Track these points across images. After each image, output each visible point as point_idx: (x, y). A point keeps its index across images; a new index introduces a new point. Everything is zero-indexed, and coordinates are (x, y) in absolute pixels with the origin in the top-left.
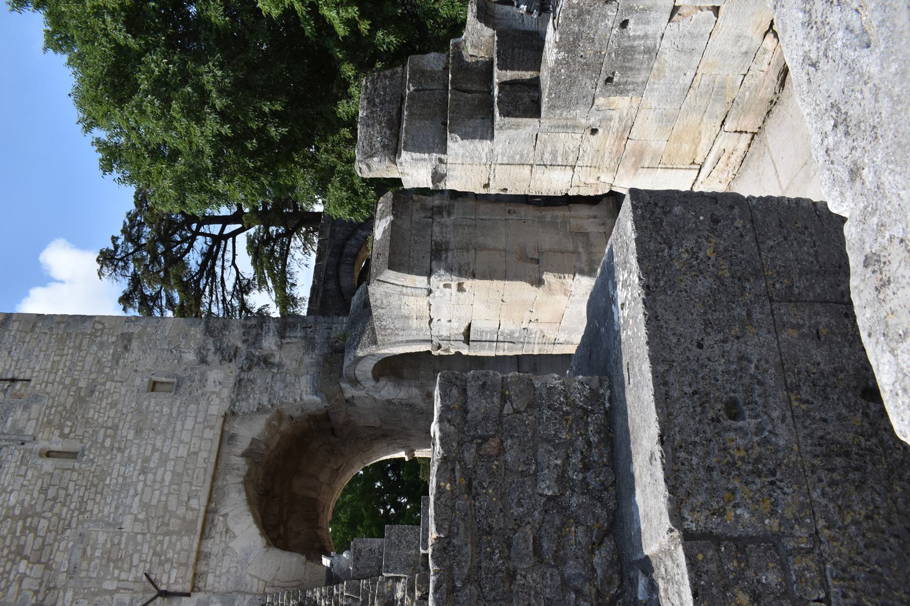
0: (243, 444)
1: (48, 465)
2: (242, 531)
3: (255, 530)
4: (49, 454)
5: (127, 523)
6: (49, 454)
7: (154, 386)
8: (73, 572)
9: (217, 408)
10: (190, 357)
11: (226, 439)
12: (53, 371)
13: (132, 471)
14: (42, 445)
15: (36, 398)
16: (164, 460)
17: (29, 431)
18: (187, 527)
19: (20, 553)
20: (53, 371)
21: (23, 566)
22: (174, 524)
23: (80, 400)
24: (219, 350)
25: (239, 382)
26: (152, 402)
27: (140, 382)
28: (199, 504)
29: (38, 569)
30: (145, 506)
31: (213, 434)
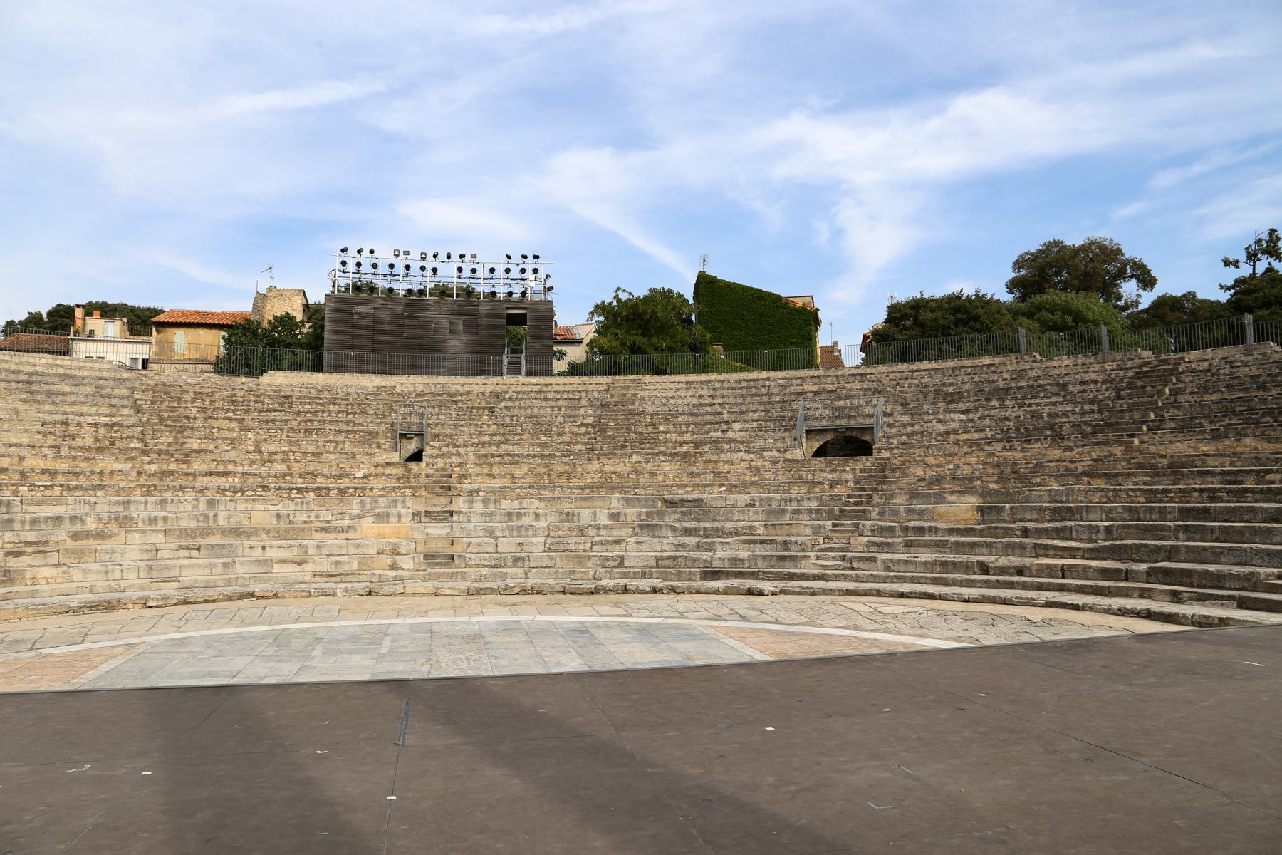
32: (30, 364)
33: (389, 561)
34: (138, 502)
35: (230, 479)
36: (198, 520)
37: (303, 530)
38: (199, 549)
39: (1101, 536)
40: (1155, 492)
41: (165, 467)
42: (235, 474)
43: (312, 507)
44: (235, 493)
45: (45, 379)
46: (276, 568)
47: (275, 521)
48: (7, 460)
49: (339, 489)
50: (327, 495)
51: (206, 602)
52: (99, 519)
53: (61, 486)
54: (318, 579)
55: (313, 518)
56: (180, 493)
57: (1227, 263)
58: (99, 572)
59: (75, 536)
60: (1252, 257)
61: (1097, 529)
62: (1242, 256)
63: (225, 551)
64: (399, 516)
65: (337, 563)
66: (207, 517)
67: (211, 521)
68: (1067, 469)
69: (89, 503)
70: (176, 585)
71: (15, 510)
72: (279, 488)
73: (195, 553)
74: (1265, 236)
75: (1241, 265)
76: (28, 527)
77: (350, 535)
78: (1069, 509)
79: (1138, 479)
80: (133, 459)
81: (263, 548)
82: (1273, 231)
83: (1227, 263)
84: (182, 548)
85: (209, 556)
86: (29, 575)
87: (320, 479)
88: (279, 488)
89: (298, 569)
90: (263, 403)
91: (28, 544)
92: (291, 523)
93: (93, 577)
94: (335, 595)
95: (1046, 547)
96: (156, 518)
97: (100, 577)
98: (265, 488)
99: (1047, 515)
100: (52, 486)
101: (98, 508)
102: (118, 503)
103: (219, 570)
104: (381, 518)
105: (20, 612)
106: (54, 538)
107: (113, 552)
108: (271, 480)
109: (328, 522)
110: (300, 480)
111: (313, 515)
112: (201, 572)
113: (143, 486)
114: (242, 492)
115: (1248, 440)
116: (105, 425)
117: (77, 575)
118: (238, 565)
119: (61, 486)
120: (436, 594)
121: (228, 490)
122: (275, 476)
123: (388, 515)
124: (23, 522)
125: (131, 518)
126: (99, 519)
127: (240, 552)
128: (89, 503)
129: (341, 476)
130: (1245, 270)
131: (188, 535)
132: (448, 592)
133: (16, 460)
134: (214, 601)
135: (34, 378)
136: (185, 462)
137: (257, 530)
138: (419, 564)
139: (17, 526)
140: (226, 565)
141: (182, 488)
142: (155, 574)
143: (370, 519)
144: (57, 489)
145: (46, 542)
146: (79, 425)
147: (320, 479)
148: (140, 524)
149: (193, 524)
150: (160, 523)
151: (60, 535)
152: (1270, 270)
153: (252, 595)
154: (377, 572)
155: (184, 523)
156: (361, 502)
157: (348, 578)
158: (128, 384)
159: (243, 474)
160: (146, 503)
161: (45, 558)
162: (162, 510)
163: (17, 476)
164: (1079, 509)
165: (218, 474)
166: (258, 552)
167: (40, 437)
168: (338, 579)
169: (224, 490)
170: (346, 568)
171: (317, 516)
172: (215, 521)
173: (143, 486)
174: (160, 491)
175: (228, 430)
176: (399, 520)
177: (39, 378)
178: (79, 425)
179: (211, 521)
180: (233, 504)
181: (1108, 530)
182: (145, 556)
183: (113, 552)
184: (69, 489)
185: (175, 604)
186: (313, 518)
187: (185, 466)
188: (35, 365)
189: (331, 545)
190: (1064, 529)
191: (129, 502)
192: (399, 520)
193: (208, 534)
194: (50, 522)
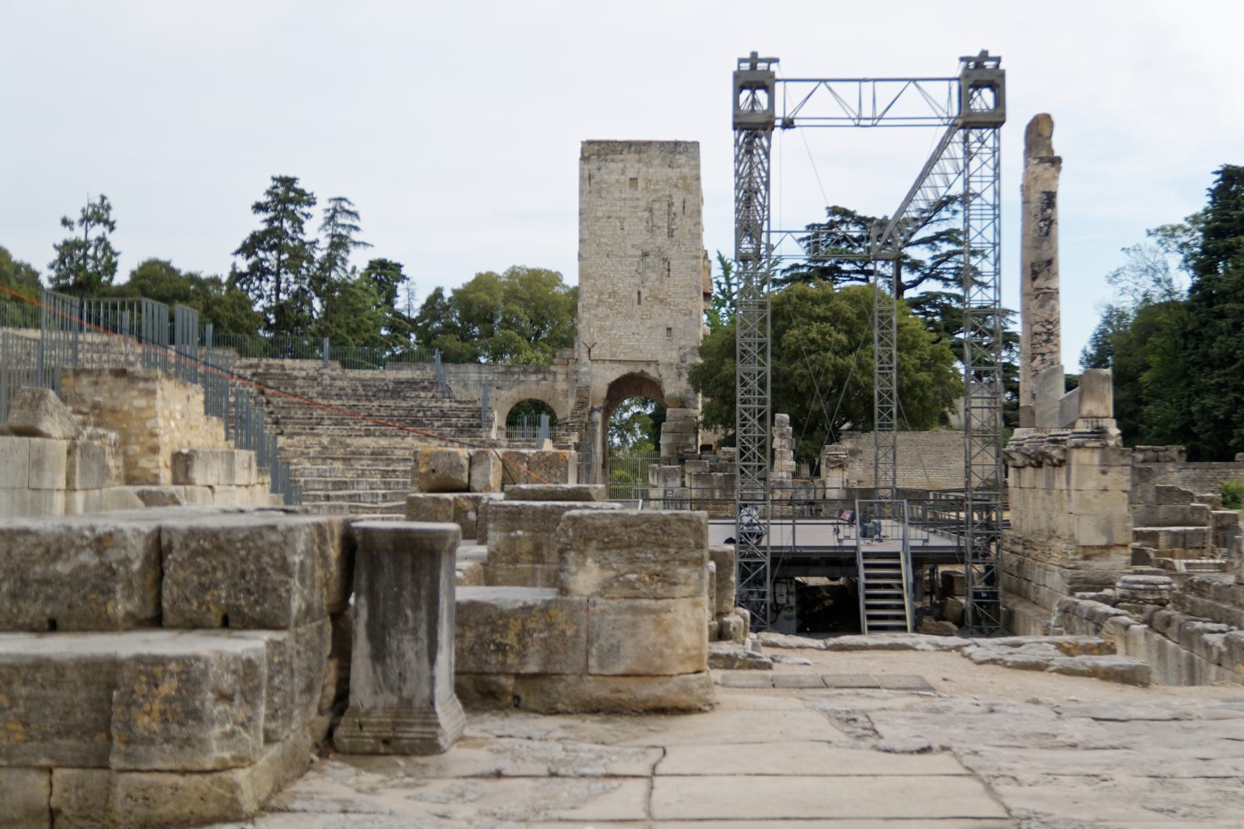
0: (647, 370)
1: (635, 296)
2: (614, 373)
3: (613, 379)
4: (639, 293)
5: (614, 332)
6: (639, 293)
7: (669, 329)
8: (596, 316)
9: (660, 358)
10: (682, 343)
11: (648, 363)
12: (675, 286)
13: (634, 329)
14: (642, 290)
15: (662, 282)
16: (638, 340)
17: (647, 284)
18: (614, 355)
19: (601, 294)
20: (675, 286)
21: (596, 296)
22: (614, 349)
23: (662, 301)
24: (685, 355)
25: (671, 364)
26: (662, 331)
27: (671, 324)
28: (622, 357)
29: (595, 302)
30: (620, 337)
31: (649, 358)
39: (380, 499)
40: (387, 472)
57: (65, 222)
60: (86, 219)
61: (377, 495)
62: (76, 216)
68: (303, 453)
74: (98, 201)
75: (76, 226)
78: (345, 482)
79: (364, 462)
82: (103, 198)
83: (65, 222)
95: (357, 507)
99: (330, 486)
115: (409, 440)
130: (78, 233)
152: (101, 240)
164: (352, 483)
181: (384, 496)
190: (354, 495)
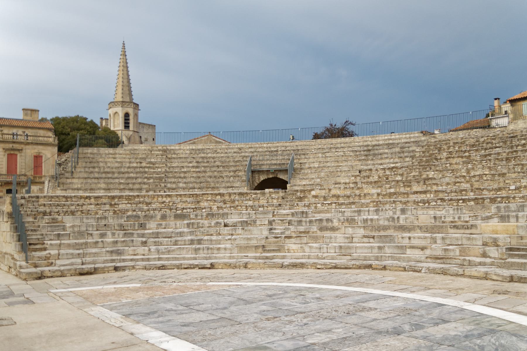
32: (377, 140)
33: (481, 251)
34: (365, 211)
35: (428, 195)
36: (389, 221)
37: (442, 227)
38: (373, 237)
41: (398, 190)
42: (431, 192)
43: (464, 211)
44: (424, 203)
45: (381, 147)
46: (409, 251)
47: (433, 221)
48: (324, 191)
49: (490, 198)
50: (483, 203)
51: (346, 268)
52: (339, 220)
53: (335, 203)
54: (429, 260)
55: (456, 219)
56: (394, 205)
58: (317, 248)
59: (321, 229)
63: (388, 239)
64: (517, 217)
65: (446, 250)
66: (393, 219)
67: (396, 221)
69: (341, 212)
70: (349, 257)
71: (309, 216)
72: (451, 200)
73: (371, 240)
76: (308, 224)
77: (473, 231)
80: (381, 187)
81: (410, 238)
84: (365, 237)
85: (379, 242)
86: (286, 248)
87: (485, 192)
88: (451, 200)
89: (421, 252)
90: (492, 143)
91: (301, 232)
92: (443, 222)
93: (314, 250)
94: (420, 271)
96: (367, 220)
97: (317, 250)
98: (442, 200)
100: (331, 203)
101: (346, 214)
102: (355, 211)
103: (376, 250)
104: (504, 218)
105: (262, 265)
106: (312, 230)
107: (331, 238)
108: (453, 194)
109: (467, 222)
110: (472, 194)
111: (456, 217)
112: (366, 251)
113: (374, 202)
114: (429, 203)
116: (389, 169)
117: (307, 249)
118: (386, 248)
119: (335, 203)
120: (486, 278)
121: (420, 202)
122: (456, 192)
123: (508, 216)
124: (306, 222)
125: (354, 220)
126: (339, 220)
127: (396, 240)
128: (341, 212)
129: (500, 189)
131: (376, 230)
132: (495, 277)
133: (327, 191)
134: (350, 268)
135: (375, 148)
136: (409, 186)
137: (414, 227)
138: (502, 254)
139: (304, 224)
140: (380, 248)
141: (394, 202)
142: (343, 251)
143: (496, 220)
144: (334, 205)
145: (309, 232)
146: (377, 170)
147: (485, 192)
148: (359, 223)
149: (386, 223)
150: (369, 223)
151: (314, 228)
153: (370, 267)
154: (467, 258)
155: (381, 222)
156: (498, 207)
157: (448, 261)
158: (399, 145)
159: (436, 191)
160: (369, 211)
161: (301, 239)
162: (377, 215)
163: (322, 199)
165: (421, 192)
166: (407, 240)
167: (353, 178)
168: (442, 261)
169: (418, 202)
170: (451, 254)
171: (459, 218)
172: (398, 221)
173: (374, 202)
174: (383, 204)
175: (456, 164)
176: (517, 221)
177: (377, 147)
178: (377, 170)
179: (396, 221)
180: (415, 211)
182: (346, 241)
183: (331, 238)
184: (339, 205)
185: (331, 268)
186: (456, 219)
187: (409, 189)
188: (379, 141)
189: (451, 238)
191: (360, 211)
192: (517, 221)
193: (387, 229)
194: (317, 222)
